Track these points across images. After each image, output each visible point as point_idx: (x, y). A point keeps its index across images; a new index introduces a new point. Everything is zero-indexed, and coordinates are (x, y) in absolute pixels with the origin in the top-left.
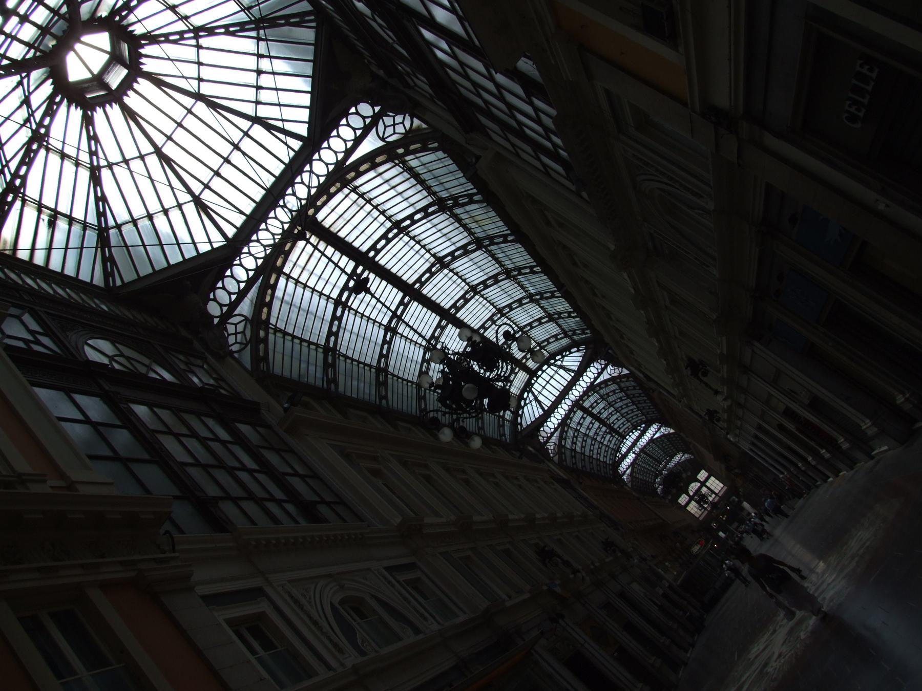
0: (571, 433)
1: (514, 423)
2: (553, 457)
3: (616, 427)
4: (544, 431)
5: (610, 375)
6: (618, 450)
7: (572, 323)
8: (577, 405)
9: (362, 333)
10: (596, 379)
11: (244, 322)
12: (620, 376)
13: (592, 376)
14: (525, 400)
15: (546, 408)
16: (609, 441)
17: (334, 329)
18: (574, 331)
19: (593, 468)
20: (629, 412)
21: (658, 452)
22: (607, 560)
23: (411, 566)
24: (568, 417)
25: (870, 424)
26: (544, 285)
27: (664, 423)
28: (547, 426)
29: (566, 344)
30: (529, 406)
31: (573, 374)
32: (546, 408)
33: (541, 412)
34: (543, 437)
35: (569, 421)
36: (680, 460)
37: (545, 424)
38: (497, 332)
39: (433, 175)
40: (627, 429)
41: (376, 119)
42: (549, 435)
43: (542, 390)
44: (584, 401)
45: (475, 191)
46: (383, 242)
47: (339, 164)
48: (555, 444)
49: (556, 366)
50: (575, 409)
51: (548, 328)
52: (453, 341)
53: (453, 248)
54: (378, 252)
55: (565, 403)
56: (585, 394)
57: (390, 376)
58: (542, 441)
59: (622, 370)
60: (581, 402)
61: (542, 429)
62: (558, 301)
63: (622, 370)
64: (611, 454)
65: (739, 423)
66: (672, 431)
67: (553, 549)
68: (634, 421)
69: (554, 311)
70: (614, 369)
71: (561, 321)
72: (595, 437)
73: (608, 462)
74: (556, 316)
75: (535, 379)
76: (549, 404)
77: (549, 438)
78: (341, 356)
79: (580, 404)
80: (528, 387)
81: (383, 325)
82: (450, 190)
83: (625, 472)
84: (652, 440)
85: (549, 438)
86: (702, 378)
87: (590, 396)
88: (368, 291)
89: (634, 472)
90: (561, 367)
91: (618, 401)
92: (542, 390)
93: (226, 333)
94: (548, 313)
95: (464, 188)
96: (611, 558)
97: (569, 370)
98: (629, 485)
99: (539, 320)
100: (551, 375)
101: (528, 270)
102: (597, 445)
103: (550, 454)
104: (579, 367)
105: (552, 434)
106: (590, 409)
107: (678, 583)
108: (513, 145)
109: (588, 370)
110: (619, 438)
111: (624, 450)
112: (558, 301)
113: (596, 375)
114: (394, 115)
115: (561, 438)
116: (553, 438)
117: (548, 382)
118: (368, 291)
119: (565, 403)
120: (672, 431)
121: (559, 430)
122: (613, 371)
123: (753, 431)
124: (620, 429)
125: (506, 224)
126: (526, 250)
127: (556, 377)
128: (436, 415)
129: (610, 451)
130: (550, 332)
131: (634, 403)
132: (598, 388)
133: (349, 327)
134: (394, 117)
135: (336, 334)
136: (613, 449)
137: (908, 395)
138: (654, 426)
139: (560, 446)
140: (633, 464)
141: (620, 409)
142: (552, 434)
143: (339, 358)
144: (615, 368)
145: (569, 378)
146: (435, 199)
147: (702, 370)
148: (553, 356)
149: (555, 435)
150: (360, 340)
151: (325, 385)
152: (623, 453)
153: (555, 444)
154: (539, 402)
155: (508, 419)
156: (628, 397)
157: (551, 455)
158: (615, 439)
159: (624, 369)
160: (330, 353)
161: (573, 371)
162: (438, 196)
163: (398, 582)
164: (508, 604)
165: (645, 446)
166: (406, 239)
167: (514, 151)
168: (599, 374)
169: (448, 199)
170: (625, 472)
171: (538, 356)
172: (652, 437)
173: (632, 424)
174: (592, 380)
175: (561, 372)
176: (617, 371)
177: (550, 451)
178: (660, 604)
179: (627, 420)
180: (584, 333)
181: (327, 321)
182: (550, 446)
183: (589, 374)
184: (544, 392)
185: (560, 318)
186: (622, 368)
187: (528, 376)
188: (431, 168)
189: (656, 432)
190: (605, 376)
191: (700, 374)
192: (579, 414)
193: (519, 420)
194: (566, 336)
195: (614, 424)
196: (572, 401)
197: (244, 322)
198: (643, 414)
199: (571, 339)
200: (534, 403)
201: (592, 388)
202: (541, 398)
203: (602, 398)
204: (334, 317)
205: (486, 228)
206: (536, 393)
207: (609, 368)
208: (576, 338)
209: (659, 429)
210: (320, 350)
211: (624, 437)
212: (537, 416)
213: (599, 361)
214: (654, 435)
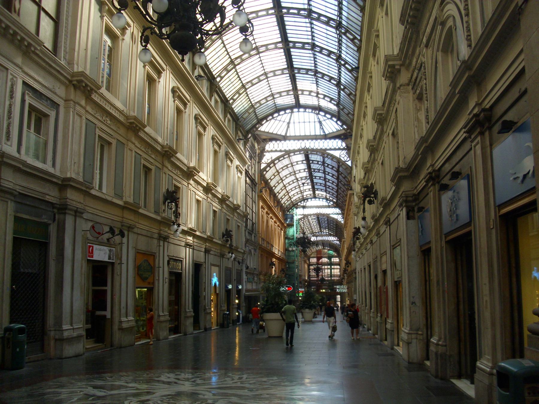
0: (286, 162)
1: (260, 122)
5: (340, 156)
10: (331, 149)
12: (344, 163)
13: (330, 146)
14: (279, 115)
15: (288, 135)
18: (344, 108)
19: (279, 193)
21: (324, 224)
22: (214, 240)
23: (55, 105)
24: (294, 151)
25: (407, 331)
30: (281, 123)
31: (322, 134)
33: (283, 134)
35: (292, 154)
36: (333, 241)
37: (278, 142)
48: (272, 158)
64: (299, 198)
65: (364, 251)
67: (179, 198)
73: (292, 200)
76: (292, 134)
77: (272, 151)
79: (307, 152)
84: (328, 216)
86: (366, 201)
87: (317, 154)
89: (301, 220)
90: (320, 122)
91: (330, 174)
96: (220, 242)
97: (323, 129)
99: (331, 78)
102: (295, 184)
104: (330, 133)
105: (276, 151)
107: (246, 293)
115: (278, 158)
117: (304, 122)
122: (343, 156)
123: (366, 264)
127: (312, 124)
131: (337, 186)
137: (440, 343)
138: (338, 209)
139: (273, 162)
140: (305, 216)
142: (276, 151)
144: (347, 156)
145: (318, 133)
147: (372, 199)
152: (307, 205)
154: (288, 127)
156: (338, 179)
161: (324, 132)
163: (23, 101)
164: (93, 192)
168: (335, 149)
171: (246, 45)
173: (326, 196)
174: (328, 148)
175: (318, 125)
176: (346, 158)
178: (218, 292)
184: (297, 125)
190: (337, 154)
191: (368, 199)
196: (305, 147)
200: (285, 124)
201: (323, 152)
202: (291, 125)
209: (337, 214)
211: (315, 197)
212: (279, 133)
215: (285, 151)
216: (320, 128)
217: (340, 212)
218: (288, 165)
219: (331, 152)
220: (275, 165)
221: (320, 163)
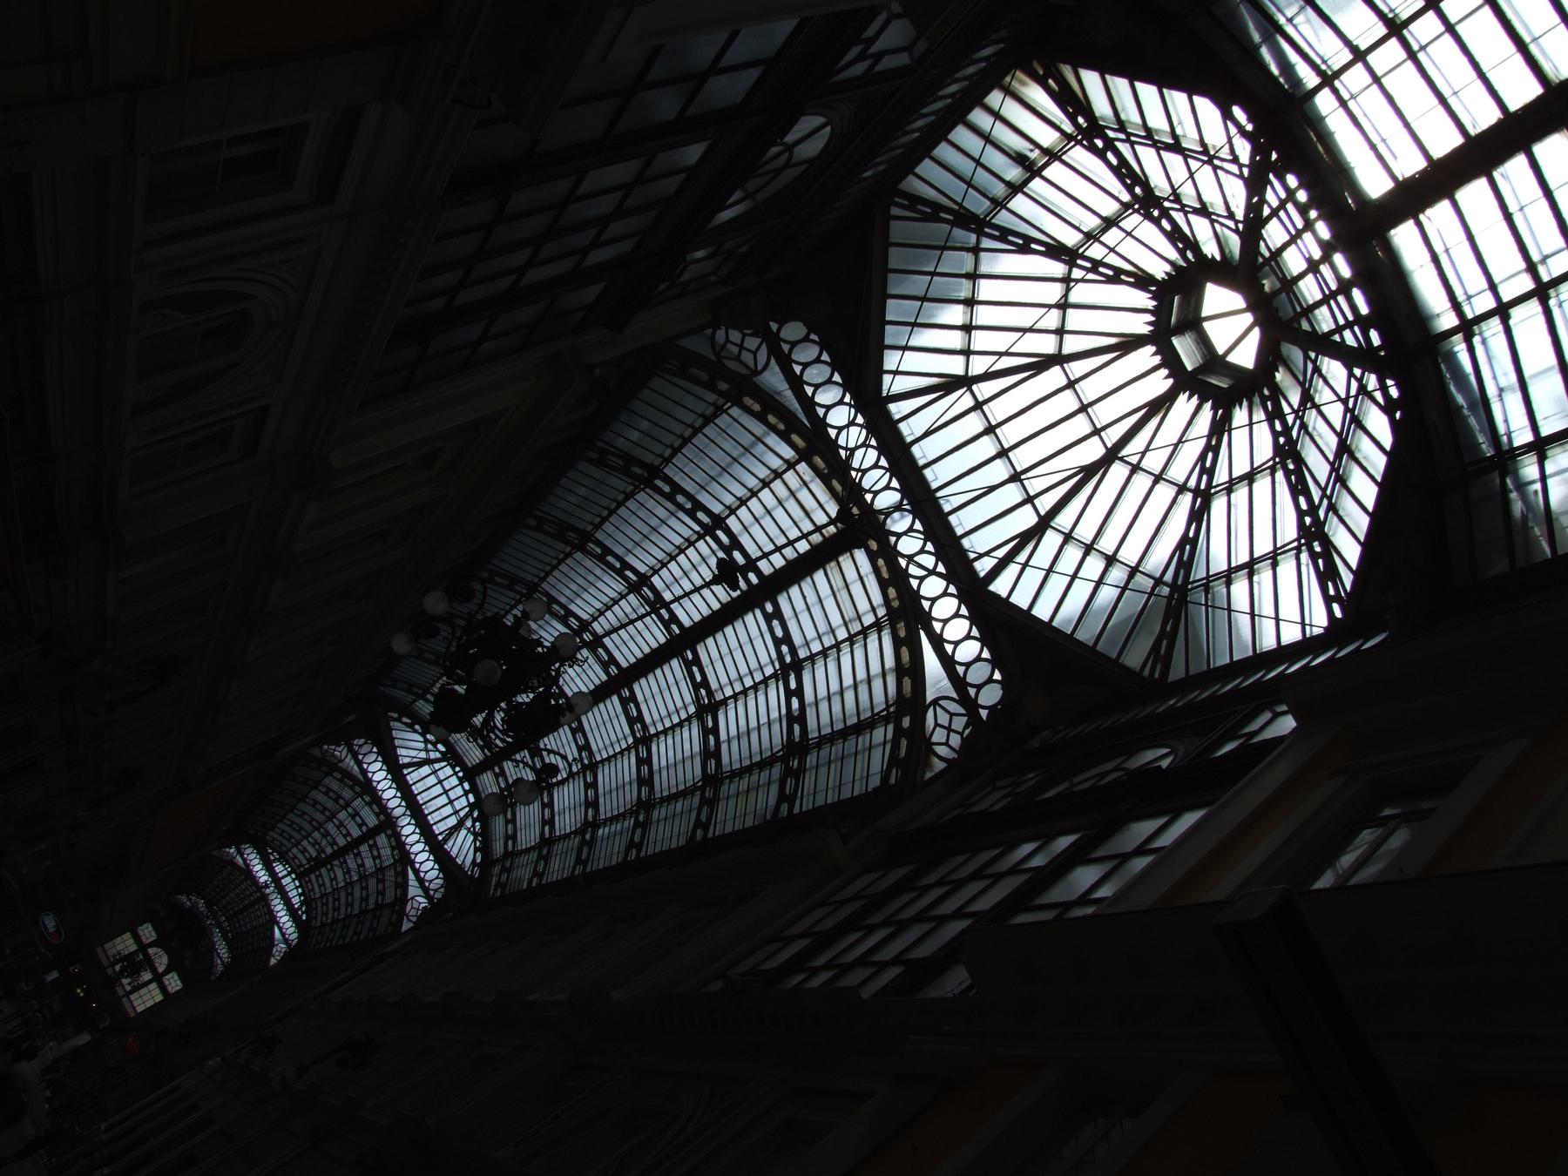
0: (347, 794)
2: (321, 748)
3: (324, 871)
4: (371, 752)
5: (413, 898)
6: (283, 859)
7: (523, 874)
8: (388, 824)
9: (654, 537)
10: (416, 872)
11: (753, 367)
12: (402, 913)
14: (435, 745)
15: (405, 772)
16: (306, 850)
17: (680, 498)
18: (509, 870)
20: (337, 903)
26: (603, 855)
27: (293, 953)
28: (375, 761)
29: (494, 847)
30: (422, 746)
32: (405, 772)
34: (361, 746)
35: (367, 799)
36: (218, 954)
37: (380, 759)
38: (564, 757)
39: (849, 756)
40: (310, 888)
41: (970, 705)
42: (360, 757)
43: (437, 777)
44: (389, 837)
45: (796, 810)
46: (779, 633)
47: (926, 619)
48: (341, 761)
49: (466, 816)
50: (382, 817)
51: (532, 830)
52: (579, 678)
53: (723, 736)
54: (768, 618)
55: (399, 806)
56: (400, 846)
57: (568, 549)
58: (355, 742)
59: (411, 921)
60: (389, 832)
61: (375, 750)
62: (567, 865)
63: (411, 921)
64: (282, 844)
66: (273, 961)
68: (319, 905)
69: (554, 853)
70: (418, 909)
71: (534, 856)
72: (322, 830)
73: (271, 833)
74: (545, 851)
75: (461, 774)
76: (411, 779)
77: (355, 755)
78: (634, 490)
80: (453, 757)
81: (652, 575)
82: (814, 772)
83: (242, 855)
84: (274, 920)
85: (355, 755)
87: (393, 849)
88: (716, 580)
90: (460, 824)
92: (437, 777)
93: (749, 332)
94: (555, 840)
95: (808, 794)
98: (216, 853)
99: (551, 822)
100: (455, 803)
101: (637, 839)
102: (308, 827)
103: (328, 745)
106: (371, 842)
108: (842, 903)
109: (436, 867)
110: (302, 869)
111: (279, 868)
112: (567, 865)
113: (422, 875)
114: (965, 736)
115: (347, 774)
116: (352, 763)
118: (716, 580)
119: (399, 806)
120: (273, 961)
121: (361, 777)
122: (416, 905)
124: (317, 877)
125: (724, 837)
126: (670, 851)
127: (448, 810)
128: (476, 601)
129: (289, 845)
130: (523, 832)
132: (399, 869)
133: (673, 522)
134: (961, 734)
135: (670, 498)
136: (289, 850)
138: (296, 935)
139: (334, 766)
140: (248, 872)
141: (349, 891)
142: (359, 763)
143: (632, 484)
144: (420, 912)
145: (437, 829)
146: (810, 742)
148: (484, 819)
149: (356, 767)
150: (646, 530)
151: (599, 444)
153: (341, 761)
154: (420, 764)
155: (417, 703)
156: (363, 912)
157: (326, 747)
158: (304, 862)
159: (411, 925)
160: (646, 474)
161: (446, 840)
162: (814, 748)
165: (268, 906)
166: (769, 671)
167: (832, 900)
168: (421, 881)
169: (802, 762)
170: (242, 855)
172: (278, 923)
173: (314, 899)
175: (453, 821)
176: (413, 912)
177: (333, 747)
179: (326, 894)
180: (499, 884)
181: (698, 492)
182: (341, 752)
183: (430, 864)
184: (432, 780)
185: (540, 857)
186: (414, 923)
187: (470, 765)
188: (859, 757)
189: (283, 934)
190: (414, 889)
192: (372, 821)
193: (405, 720)
194: (507, 854)
195: (329, 870)
196: (397, 818)
197: (753, 367)
198: (323, 925)
199: (498, 860)
200: (423, 755)
201: (404, 858)
202: (426, 770)
203: (381, 870)
204: (699, 506)
205: (732, 802)
206: (437, 766)
207: (422, 901)
208: (496, 870)
209: (286, 941)
210: (657, 462)
212: (401, 751)
213: (442, 890)
214: (280, 929)
215: (370, 781)
216: (451, 828)
217: (295, 942)
218: (343, 799)
219: (411, 876)
220: (330, 774)
221: (377, 861)
